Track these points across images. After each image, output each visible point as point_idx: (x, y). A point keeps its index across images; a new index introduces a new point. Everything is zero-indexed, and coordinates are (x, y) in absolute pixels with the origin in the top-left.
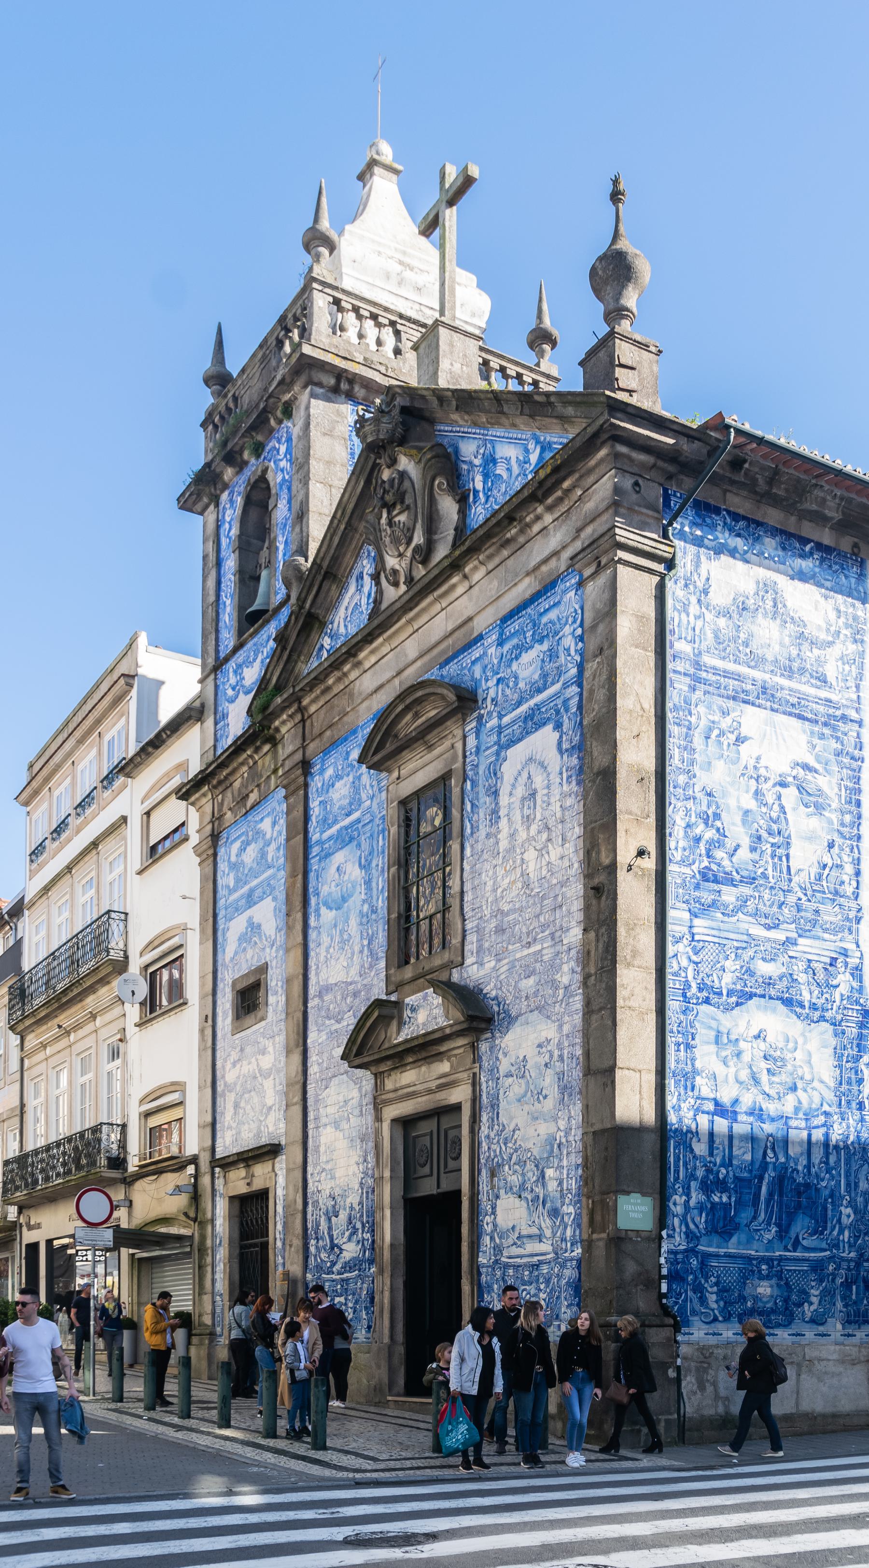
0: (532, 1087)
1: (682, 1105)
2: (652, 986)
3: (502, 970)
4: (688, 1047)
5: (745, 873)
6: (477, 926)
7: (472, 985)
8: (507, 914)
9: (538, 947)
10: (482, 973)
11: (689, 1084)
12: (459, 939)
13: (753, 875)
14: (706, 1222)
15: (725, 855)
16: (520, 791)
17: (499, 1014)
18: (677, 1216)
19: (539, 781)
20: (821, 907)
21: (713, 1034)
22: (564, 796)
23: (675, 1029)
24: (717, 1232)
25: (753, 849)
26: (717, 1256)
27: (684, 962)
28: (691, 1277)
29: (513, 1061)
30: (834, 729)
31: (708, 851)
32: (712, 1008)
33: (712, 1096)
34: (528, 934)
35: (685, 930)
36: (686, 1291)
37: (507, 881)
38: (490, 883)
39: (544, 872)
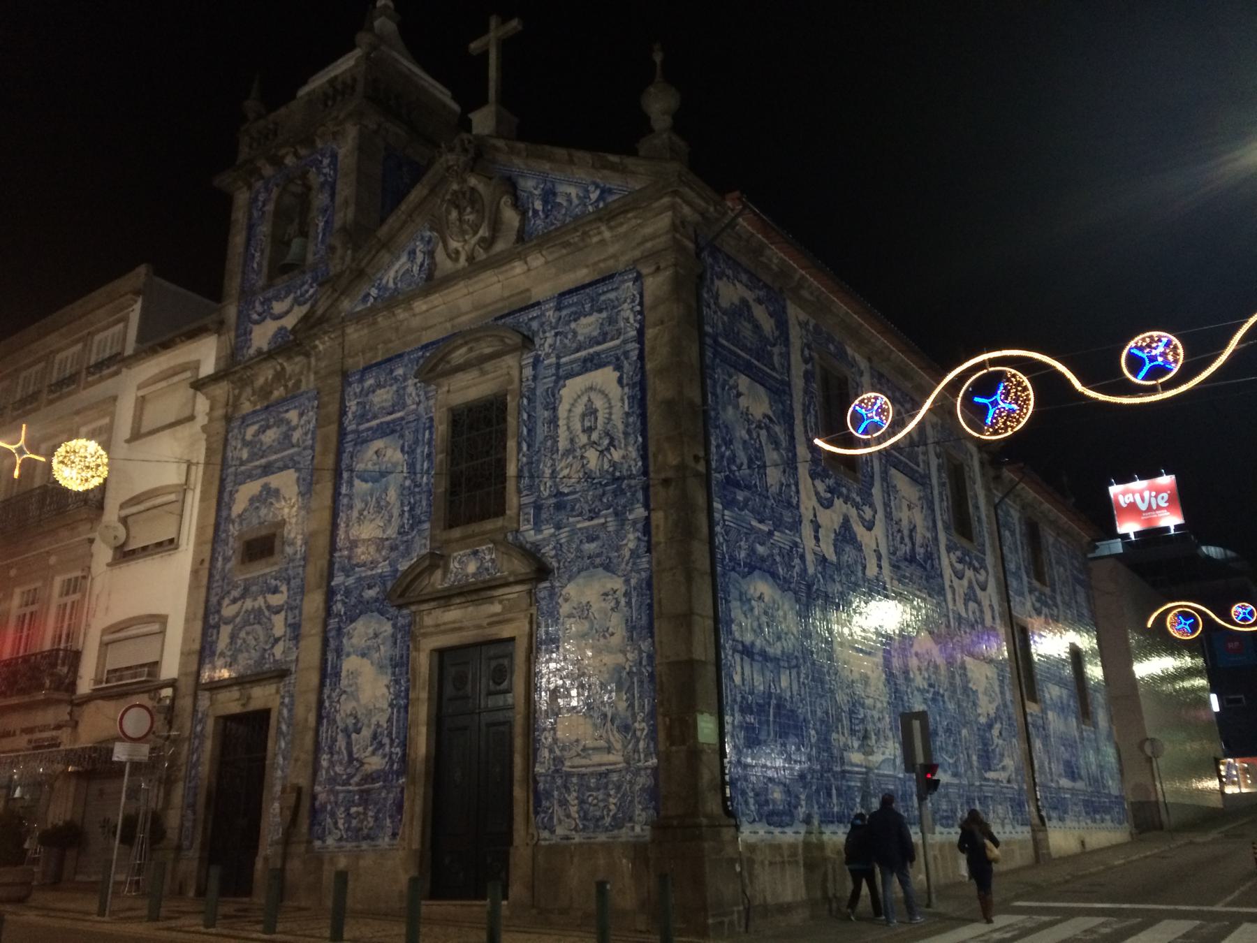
0: (596, 626)
2: (707, 555)
3: (562, 536)
4: (726, 600)
6: (534, 502)
7: (528, 546)
8: (568, 494)
9: (602, 520)
10: (540, 537)
16: (580, 409)
17: (559, 568)
19: (599, 403)
20: (784, 512)
21: (737, 593)
22: (627, 414)
25: (749, 467)
29: (575, 606)
34: (590, 511)
37: (566, 472)
38: (548, 472)
39: (606, 467)
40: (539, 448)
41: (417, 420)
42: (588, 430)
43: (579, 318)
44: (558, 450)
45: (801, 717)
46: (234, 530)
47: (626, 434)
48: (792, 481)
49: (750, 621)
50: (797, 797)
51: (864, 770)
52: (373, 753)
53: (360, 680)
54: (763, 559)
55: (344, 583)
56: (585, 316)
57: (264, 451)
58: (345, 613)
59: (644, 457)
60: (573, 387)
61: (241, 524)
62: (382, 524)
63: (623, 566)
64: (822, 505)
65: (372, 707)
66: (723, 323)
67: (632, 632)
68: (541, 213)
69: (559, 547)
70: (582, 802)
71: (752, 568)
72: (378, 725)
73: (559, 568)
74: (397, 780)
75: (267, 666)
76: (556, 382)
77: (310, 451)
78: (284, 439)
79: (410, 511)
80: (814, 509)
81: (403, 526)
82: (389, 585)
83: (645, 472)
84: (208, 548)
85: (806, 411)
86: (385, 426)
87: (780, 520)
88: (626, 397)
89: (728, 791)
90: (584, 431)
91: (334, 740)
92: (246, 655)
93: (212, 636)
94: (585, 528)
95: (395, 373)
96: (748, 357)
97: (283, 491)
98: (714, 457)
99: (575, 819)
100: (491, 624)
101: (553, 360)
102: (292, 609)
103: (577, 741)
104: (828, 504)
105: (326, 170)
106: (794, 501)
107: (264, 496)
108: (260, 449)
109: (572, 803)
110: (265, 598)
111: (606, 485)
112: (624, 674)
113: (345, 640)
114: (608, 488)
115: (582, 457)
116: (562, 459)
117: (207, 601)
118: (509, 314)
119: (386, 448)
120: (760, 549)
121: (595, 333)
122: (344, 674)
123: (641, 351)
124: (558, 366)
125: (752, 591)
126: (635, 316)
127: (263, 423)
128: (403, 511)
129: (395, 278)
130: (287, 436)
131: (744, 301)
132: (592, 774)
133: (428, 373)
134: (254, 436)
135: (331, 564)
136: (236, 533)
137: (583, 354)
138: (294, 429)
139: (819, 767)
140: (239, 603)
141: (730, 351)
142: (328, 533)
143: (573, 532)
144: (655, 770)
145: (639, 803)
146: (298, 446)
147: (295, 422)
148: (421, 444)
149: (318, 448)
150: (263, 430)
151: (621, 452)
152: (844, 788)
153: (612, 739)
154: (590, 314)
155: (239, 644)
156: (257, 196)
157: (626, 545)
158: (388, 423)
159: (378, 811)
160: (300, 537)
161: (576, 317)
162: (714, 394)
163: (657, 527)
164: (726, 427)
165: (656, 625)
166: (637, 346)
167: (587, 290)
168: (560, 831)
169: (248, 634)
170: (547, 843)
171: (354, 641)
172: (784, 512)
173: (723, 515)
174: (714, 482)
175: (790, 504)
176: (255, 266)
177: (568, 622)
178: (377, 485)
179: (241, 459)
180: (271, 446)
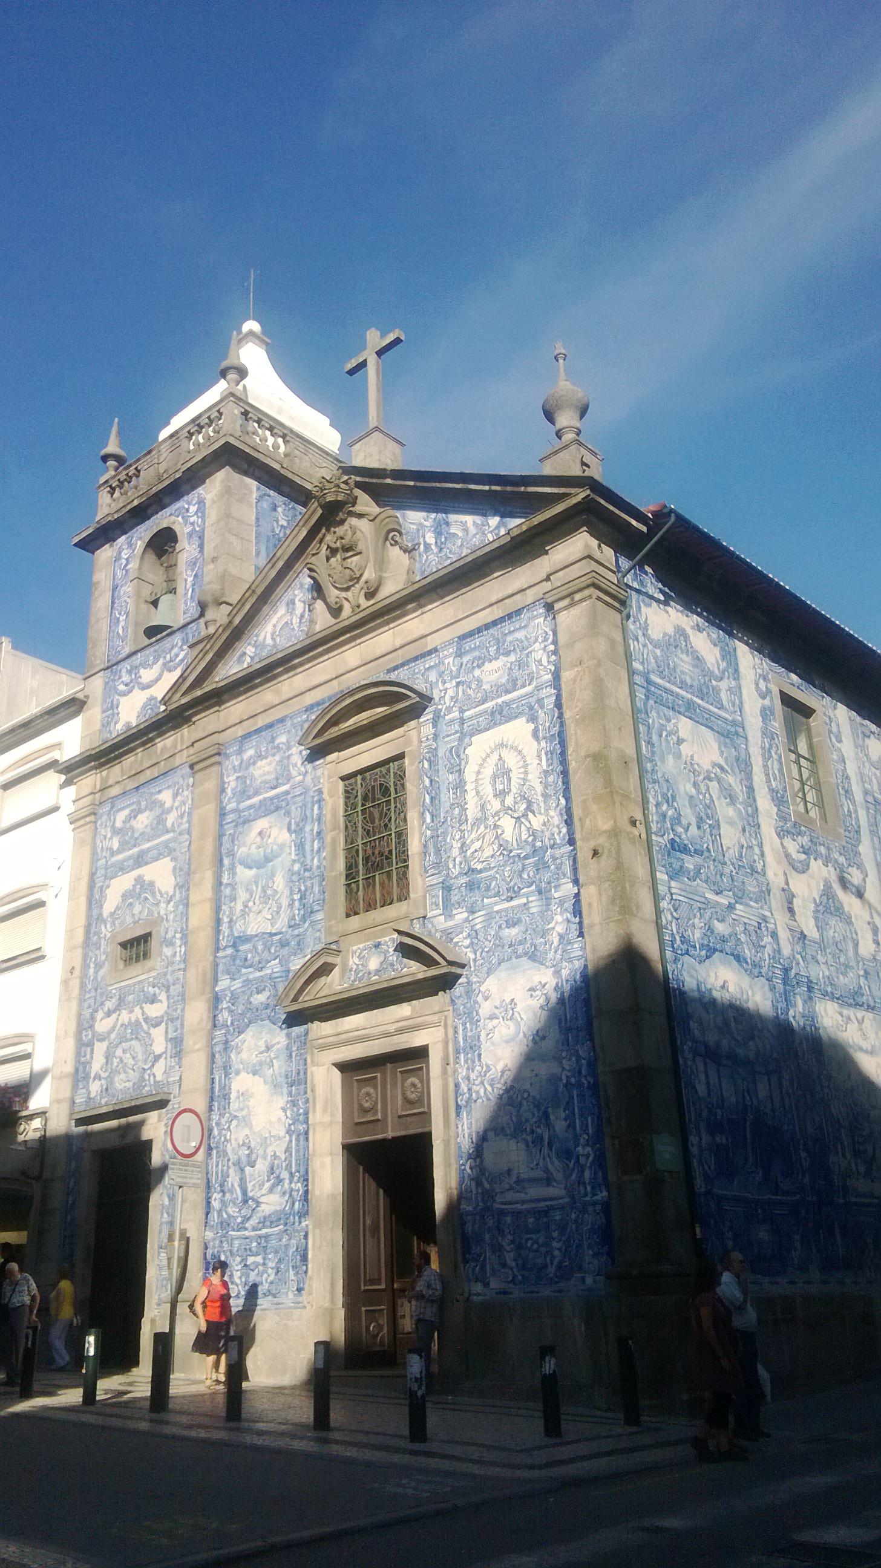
3: (477, 921)
5: (698, 847)
7: (438, 935)
8: (481, 871)
9: (524, 900)
10: (451, 923)
12: (420, 893)
16: (489, 770)
19: (512, 761)
22: (546, 772)
25: (699, 828)
27: (669, 918)
28: (712, 1222)
29: (498, 1004)
30: (732, 740)
31: (672, 825)
33: (702, 1039)
34: (508, 890)
37: (477, 845)
38: (457, 845)
40: (446, 818)
41: (305, 793)
42: (501, 794)
43: (483, 664)
44: (467, 820)
46: (106, 931)
47: (545, 796)
51: (876, 1201)
52: (271, 1190)
53: (252, 1103)
54: (724, 940)
55: (230, 987)
56: (491, 661)
57: (136, 839)
58: (232, 1023)
59: (569, 823)
60: (479, 746)
61: (113, 923)
62: (270, 917)
63: (551, 955)
65: (267, 1135)
66: (656, 658)
67: (567, 1034)
68: (433, 547)
69: (474, 934)
70: (519, 1247)
71: (711, 951)
72: (275, 1156)
73: (475, 960)
74: (300, 1223)
75: (147, 1089)
76: (461, 740)
77: (187, 836)
78: (158, 823)
79: (301, 898)
80: (785, 874)
81: (293, 918)
82: (281, 987)
83: (572, 842)
84: (79, 951)
85: (766, 754)
86: (269, 803)
87: (743, 891)
88: (543, 752)
89: (698, 1230)
90: (495, 796)
91: (226, 1176)
92: (123, 1076)
93: (85, 1056)
94: (506, 910)
95: (277, 742)
96: (689, 696)
97: (157, 884)
98: (654, 818)
99: (512, 1269)
100: (400, 1031)
101: (455, 714)
102: (172, 1020)
103: (509, 1172)
104: (803, 868)
105: (192, 520)
106: (759, 868)
107: (138, 890)
108: (132, 837)
109: (508, 1248)
110: (142, 1008)
111: (526, 857)
112: (561, 1088)
113: (233, 1056)
114: (528, 861)
115: (496, 826)
116: (472, 830)
117: (80, 1015)
118: (403, 665)
119: (270, 827)
120: (720, 927)
121: (504, 681)
122: (233, 1096)
123: (559, 697)
124: (462, 721)
125: (712, 980)
126: (549, 657)
127: (134, 807)
128: (293, 900)
129: (273, 634)
130: (160, 821)
131: (681, 632)
132: (528, 1211)
133: (314, 738)
134: (124, 822)
135: (216, 965)
136: (109, 935)
137: (490, 705)
138: (169, 811)
139: (815, 1199)
140: (114, 1016)
141: (666, 690)
142: (210, 929)
143: (490, 917)
144: (606, 1206)
145: (589, 1247)
146: (174, 831)
147: (167, 805)
148: (309, 820)
149: (195, 833)
150: (133, 815)
151: (541, 818)
153: (550, 1167)
154: (497, 659)
155: (115, 1064)
156: (120, 553)
157: (554, 928)
158: (272, 799)
159: (280, 1261)
160: (178, 936)
161: (480, 662)
162: (649, 742)
163: (590, 905)
164: (667, 781)
165: (595, 1025)
166: (553, 691)
167: (491, 631)
168: (494, 1284)
169: (124, 1052)
170: (481, 1298)
171: (244, 1055)
173: (670, 888)
174: (655, 848)
175: (754, 871)
176: (121, 632)
177: (491, 1024)
178: (262, 871)
179: (111, 849)
180: (143, 833)
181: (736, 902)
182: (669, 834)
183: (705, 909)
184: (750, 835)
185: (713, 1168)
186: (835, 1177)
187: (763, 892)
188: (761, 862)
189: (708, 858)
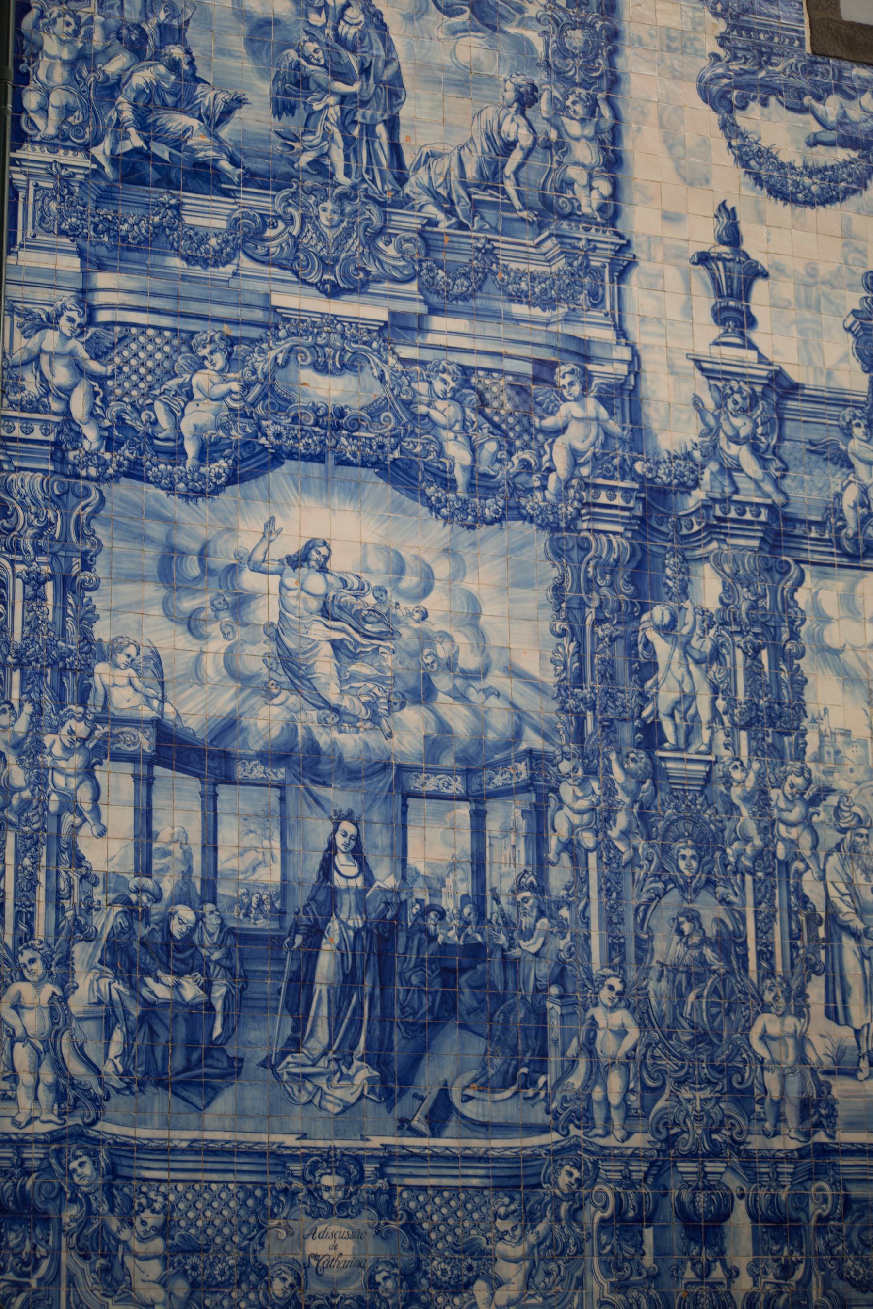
1: (48, 740)
5: (259, 165)
11: (70, 682)
13: (284, 168)
14: (126, 1054)
15: (195, 123)
18: (25, 1038)
23: (27, 544)
24: (161, 1083)
26: (164, 1151)
27: (61, 375)
28: (70, 1214)
32: (151, 489)
33: (147, 713)
35: (67, 298)
36: (55, 1255)
45: (544, 969)
48: (574, 128)
49: (217, 645)
50: (472, 1249)
64: (778, 193)
80: (728, 213)
87: (486, 275)
152: (815, 1209)
172: (502, 243)
173: (84, 293)
181: (434, 311)
182: (120, 135)
183: (252, 341)
184: (560, 108)
185: (108, 1068)
186: (772, 1081)
187: (597, 273)
188: (604, 187)
189: (311, 191)
